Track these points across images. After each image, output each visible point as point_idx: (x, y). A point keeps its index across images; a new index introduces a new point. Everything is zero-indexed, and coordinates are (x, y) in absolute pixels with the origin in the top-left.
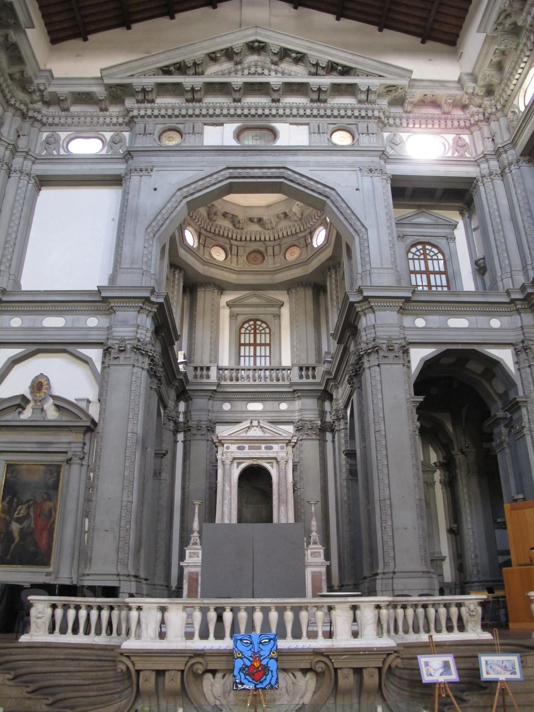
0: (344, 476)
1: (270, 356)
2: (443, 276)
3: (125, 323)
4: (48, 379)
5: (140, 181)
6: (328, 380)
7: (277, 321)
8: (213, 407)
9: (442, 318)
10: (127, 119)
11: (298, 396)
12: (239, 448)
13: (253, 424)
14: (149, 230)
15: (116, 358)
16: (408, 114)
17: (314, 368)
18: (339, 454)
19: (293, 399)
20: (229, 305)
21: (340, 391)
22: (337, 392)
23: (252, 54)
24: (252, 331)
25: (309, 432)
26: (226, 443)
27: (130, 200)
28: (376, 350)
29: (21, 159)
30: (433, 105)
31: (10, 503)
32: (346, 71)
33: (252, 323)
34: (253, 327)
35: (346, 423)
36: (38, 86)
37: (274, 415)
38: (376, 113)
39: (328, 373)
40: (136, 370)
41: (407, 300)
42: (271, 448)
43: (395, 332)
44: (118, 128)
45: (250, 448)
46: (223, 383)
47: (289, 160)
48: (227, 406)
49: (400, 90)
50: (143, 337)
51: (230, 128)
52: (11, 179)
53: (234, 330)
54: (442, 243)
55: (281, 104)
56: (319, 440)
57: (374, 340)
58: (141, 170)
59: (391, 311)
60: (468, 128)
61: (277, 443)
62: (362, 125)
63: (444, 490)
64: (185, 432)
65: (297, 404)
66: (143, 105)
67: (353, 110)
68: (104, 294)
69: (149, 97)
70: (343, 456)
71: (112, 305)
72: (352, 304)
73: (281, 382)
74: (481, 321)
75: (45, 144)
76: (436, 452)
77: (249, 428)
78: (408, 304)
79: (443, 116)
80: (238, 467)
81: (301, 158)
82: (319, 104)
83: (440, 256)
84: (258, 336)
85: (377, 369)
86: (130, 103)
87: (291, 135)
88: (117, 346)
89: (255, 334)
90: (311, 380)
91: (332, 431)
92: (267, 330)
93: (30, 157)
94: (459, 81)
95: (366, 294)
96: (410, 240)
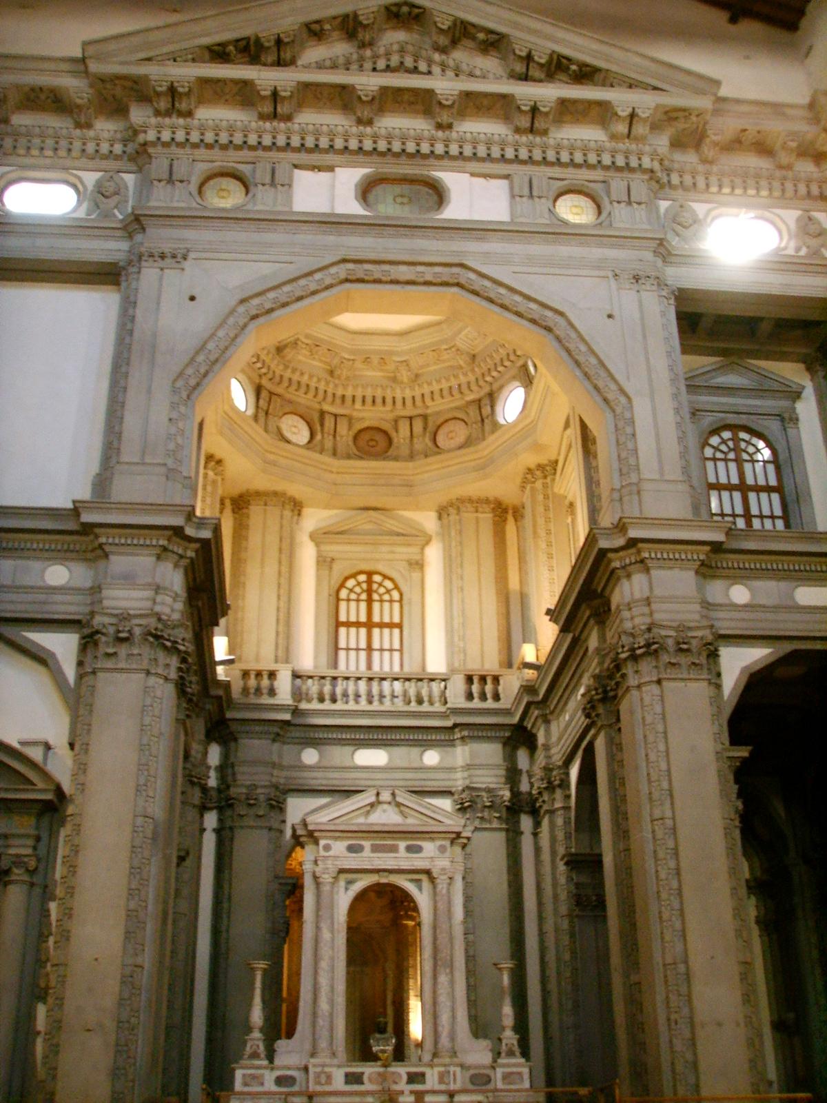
0: (564, 909)
1: (401, 650)
3: (129, 579)
5: (161, 279)
6: (529, 704)
7: (416, 575)
8: (280, 756)
9: (783, 585)
10: (131, 148)
11: (462, 738)
12: (351, 849)
13: (381, 798)
14: (180, 384)
15: (108, 655)
16: (708, 166)
17: (496, 679)
18: (553, 862)
19: (451, 743)
20: (318, 537)
21: (555, 728)
22: (548, 732)
23: (394, 28)
24: (364, 596)
25: (486, 814)
26: (326, 838)
28: (652, 649)
32: (586, 74)
33: (362, 578)
34: (364, 586)
35: (568, 797)
37: (410, 775)
38: (646, 162)
39: (529, 689)
40: (152, 680)
41: (716, 547)
42: (419, 849)
43: (690, 613)
44: (112, 164)
45: (375, 849)
46: (304, 706)
47: (472, 251)
48: (310, 756)
49: (694, 119)
50: (167, 610)
51: (349, 177)
53: (325, 594)
54: (773, 427)
55: (454, 135)
56: (507, 830)
57: (649, 630)
58: (163, 256)
59: (681, 569)
61: (432, 839)
62: (618, 184)
63: (766, 939)
64: (220, 810)
65: (461, 754)
66: (167, 121)
67: (599, 151)
68: (87, 517)
69: (183, 106)
70: (562, 867)
71: (103, 540)
72: (603, 553)
73: (426, 707)
77: (372, 805)
78: (716, 559)
79: (778, 173)
80: (347, 889)
81: (495, 246)
82: (531, 137)
84: (376, 606)
85: (655, 689)
87: (474, 197)
88: (111, 630)
89: (370, 601)
90: (490, 704)
91: (535, 813)
92: (396, 595)
94: (812, 106)
95: (633, 533)
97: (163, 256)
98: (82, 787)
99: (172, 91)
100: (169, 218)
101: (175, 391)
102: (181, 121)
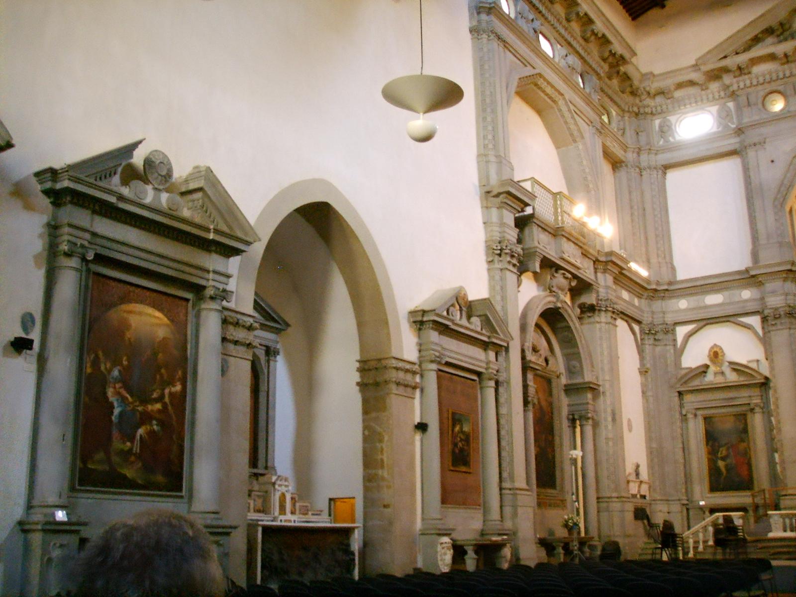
3: (773, 292)
4: (721, 349)
14: (776, 203)
15: (773, 325)
27: (752, 177)
29: (646, 155)
31: (712, 446)
36: (644, 88)
52: (643, 177)
58: (755, 145)
66: (741, 78)
68: (753, 273)
75: (660, 133)
86: (727, 79)
88: (772, 314)
93: (653, 151)
97: (755, 145)
98: (774, 376)
99: (739, 68)
100: (752, 126)
101: (775, 207)
102: (746, 77)
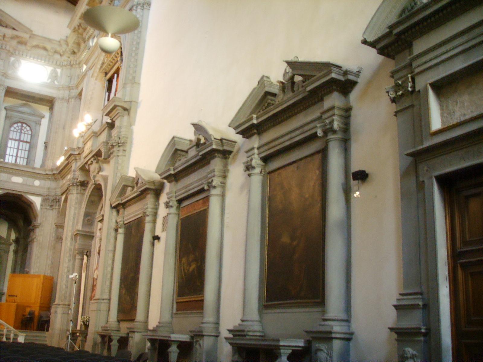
2: (28, 145)
9: (9, 175)
30: (43, 49)
54: (33, 125)
60: (61, 66)
63: (14, 256)
74: (29, 180)
76: (15, 233)
83: (30, 132)
94: (60, 42)
96: (15, 120)
